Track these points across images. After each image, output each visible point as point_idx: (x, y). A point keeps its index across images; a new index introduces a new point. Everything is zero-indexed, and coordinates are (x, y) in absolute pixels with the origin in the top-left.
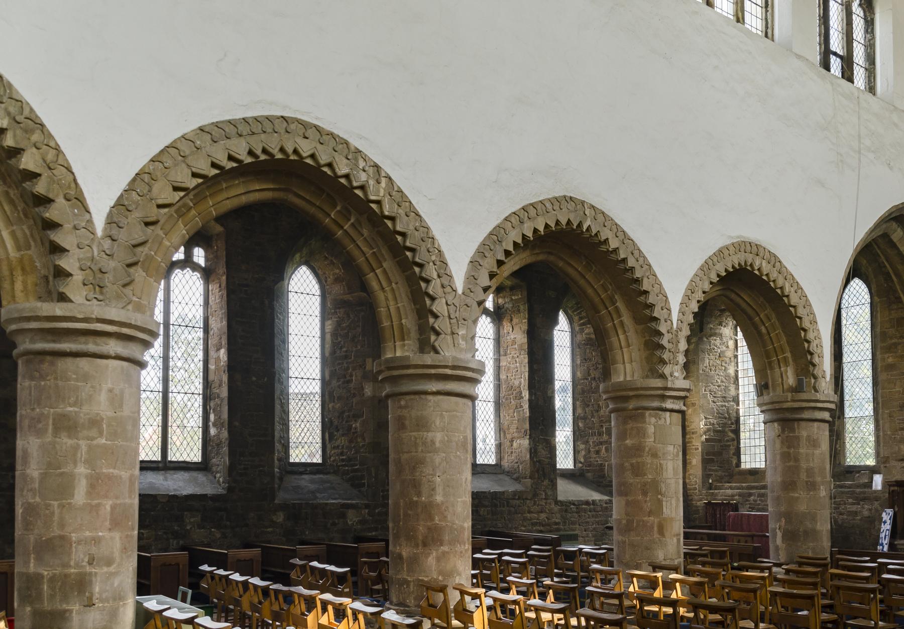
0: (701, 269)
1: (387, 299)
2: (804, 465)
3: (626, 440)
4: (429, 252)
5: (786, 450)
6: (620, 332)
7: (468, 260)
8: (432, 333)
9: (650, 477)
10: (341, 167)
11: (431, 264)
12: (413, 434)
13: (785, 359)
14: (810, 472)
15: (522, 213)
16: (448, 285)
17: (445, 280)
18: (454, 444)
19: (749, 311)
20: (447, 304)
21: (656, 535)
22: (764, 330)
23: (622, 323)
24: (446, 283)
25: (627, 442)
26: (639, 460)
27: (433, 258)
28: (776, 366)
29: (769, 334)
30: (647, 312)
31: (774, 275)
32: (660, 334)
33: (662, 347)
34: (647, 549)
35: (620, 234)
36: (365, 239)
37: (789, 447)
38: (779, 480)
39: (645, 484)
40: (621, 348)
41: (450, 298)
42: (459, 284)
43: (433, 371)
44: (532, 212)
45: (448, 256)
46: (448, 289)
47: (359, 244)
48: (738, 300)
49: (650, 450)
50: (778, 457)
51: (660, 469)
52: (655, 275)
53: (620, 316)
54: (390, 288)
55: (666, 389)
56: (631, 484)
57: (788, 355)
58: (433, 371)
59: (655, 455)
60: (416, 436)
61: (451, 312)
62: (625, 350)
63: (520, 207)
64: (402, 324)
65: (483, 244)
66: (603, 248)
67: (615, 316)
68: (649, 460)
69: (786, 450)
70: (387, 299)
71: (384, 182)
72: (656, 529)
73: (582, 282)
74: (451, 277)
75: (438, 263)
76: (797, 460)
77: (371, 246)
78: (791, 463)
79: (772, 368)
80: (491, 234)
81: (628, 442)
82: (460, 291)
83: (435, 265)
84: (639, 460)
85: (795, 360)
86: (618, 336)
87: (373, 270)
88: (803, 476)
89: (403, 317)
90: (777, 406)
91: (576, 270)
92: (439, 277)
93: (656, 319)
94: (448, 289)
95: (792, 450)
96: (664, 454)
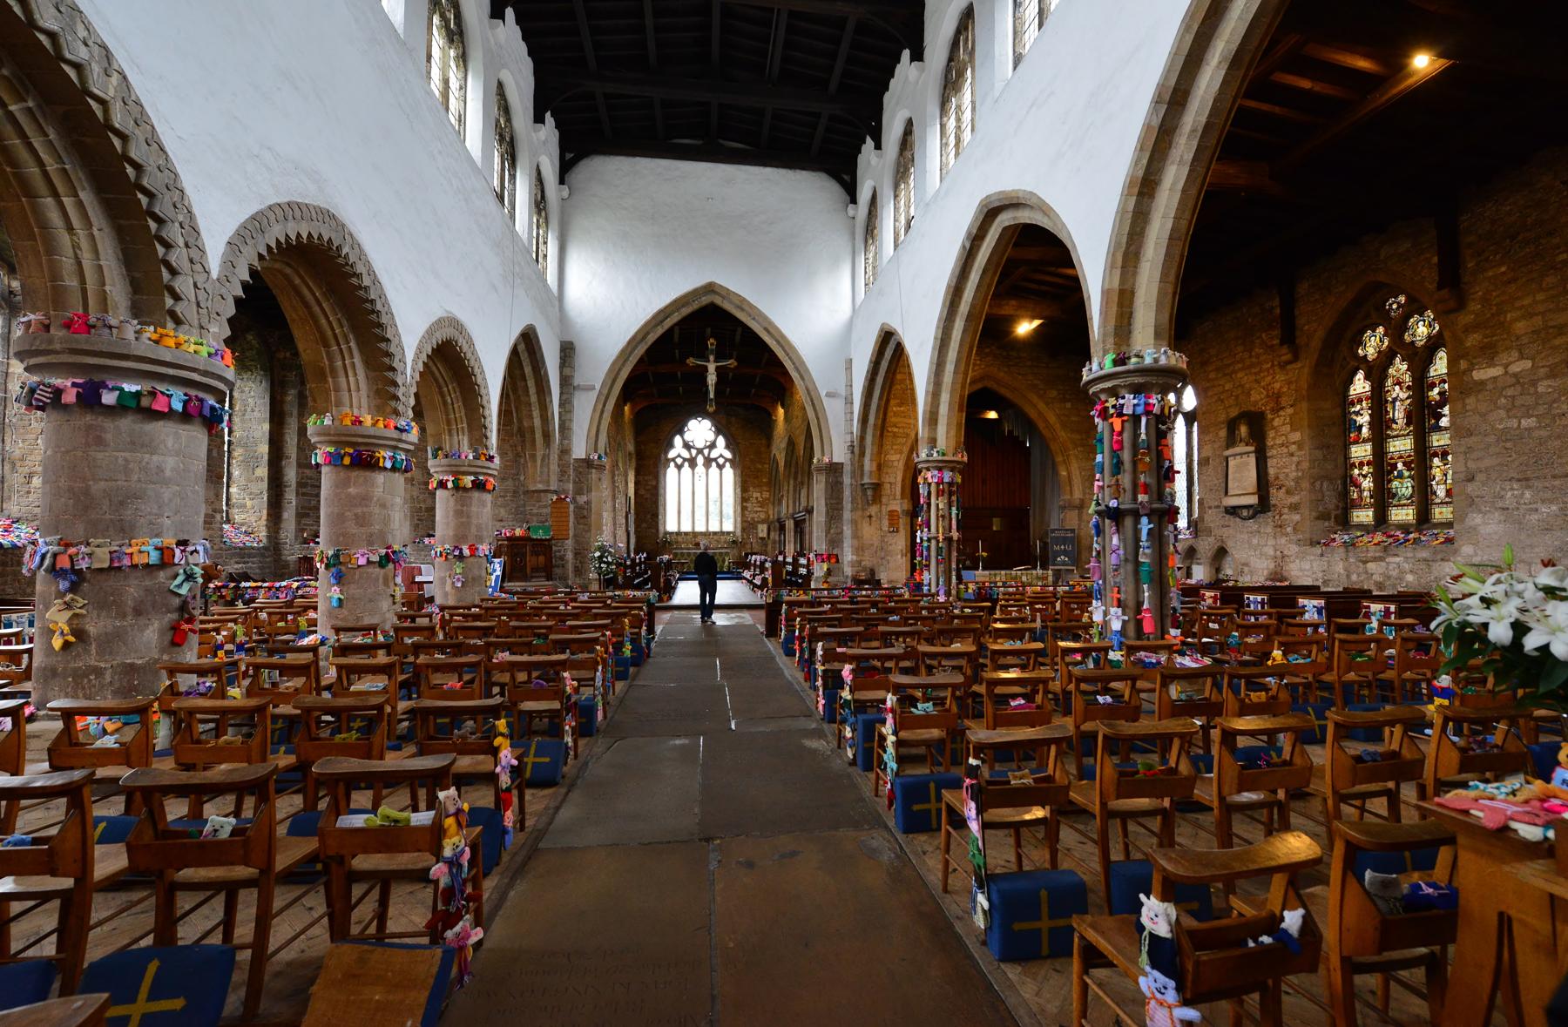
0: (427, 332)
1: (76, 247)
2: (474, 521)
3: (350, 487)
4: (175, 207)
5: (459, 507)
6: (350, 373)
7: (226, 239)
8: (168, 319)
9: (377, 527)
10: (45, 16)
11: (177, 225)
12: (123, 454)
13: (463, 428)
14: (479, 528)
15: (286, 208)
16: (198, 260)
17: (194, 253)
18: (192, 475)
19: (441, 380)
20: (195, 286)
21: (381, 587)
22: (449, 401)
23: (353, 365)
24: (196, 258)
25: (350, 490)
26: (365, 509)
27: (181, 218)
28: (455, 434)
29: (453, 404)
30: (386, 360)
31: (469, 355)
32: (395, 384)
33: (397, 399)
34: (371, 601)
35: (371, 273)
36: (50, 141)
37: (463, 506)
38: (451, 533)
39: (371, 535)
40: (350, 390)
41: (200, 279)
42: (214, 265)
43: (171, 372)
44: (298, 213)
45: (202, 224)
46: (198, 267)
47: (36, 145)
48: (434, 368)
49: (378, 500)
50: (451, 513)
51: (387, 521)
52: (396, 326)
53: (352, 357)
54: (86, 232)
55: (400, 440)
56: (354, 535)
57: (465, 425)
58: (171, 372)
59: (383, 506)
60: (129, 458)
61: (200, 298)
62: (354, 394)
63: (286, 200)
64: (105, 291)
65: (244, 226)
66: (354, 281)
67: (346, 357)
68: (377, 510)
69: (459, 507)
70: (76, 247)
71: (115, 79)
72: (381, 580)
73: (316, 309)
74: (204, 252)
75: (186, 227)
76: (468, 517)
77: (60, 157)
78: (464, 520)
79: (451, 435)
80: (253, 218)
81: (351, 490)
82: (214, 274)
83: (182, 228)
84: (365, 509)
85: (470, 431)
86: (347, 376)
87: (55, 194)
88: (474, 530)
89: (108, 281)
90: (454, 469)
91: (314, 294)
92: (187, 246)
93: (394, 370)
94: (198, 267)
95: (465, 508)
96: (392, 505)
